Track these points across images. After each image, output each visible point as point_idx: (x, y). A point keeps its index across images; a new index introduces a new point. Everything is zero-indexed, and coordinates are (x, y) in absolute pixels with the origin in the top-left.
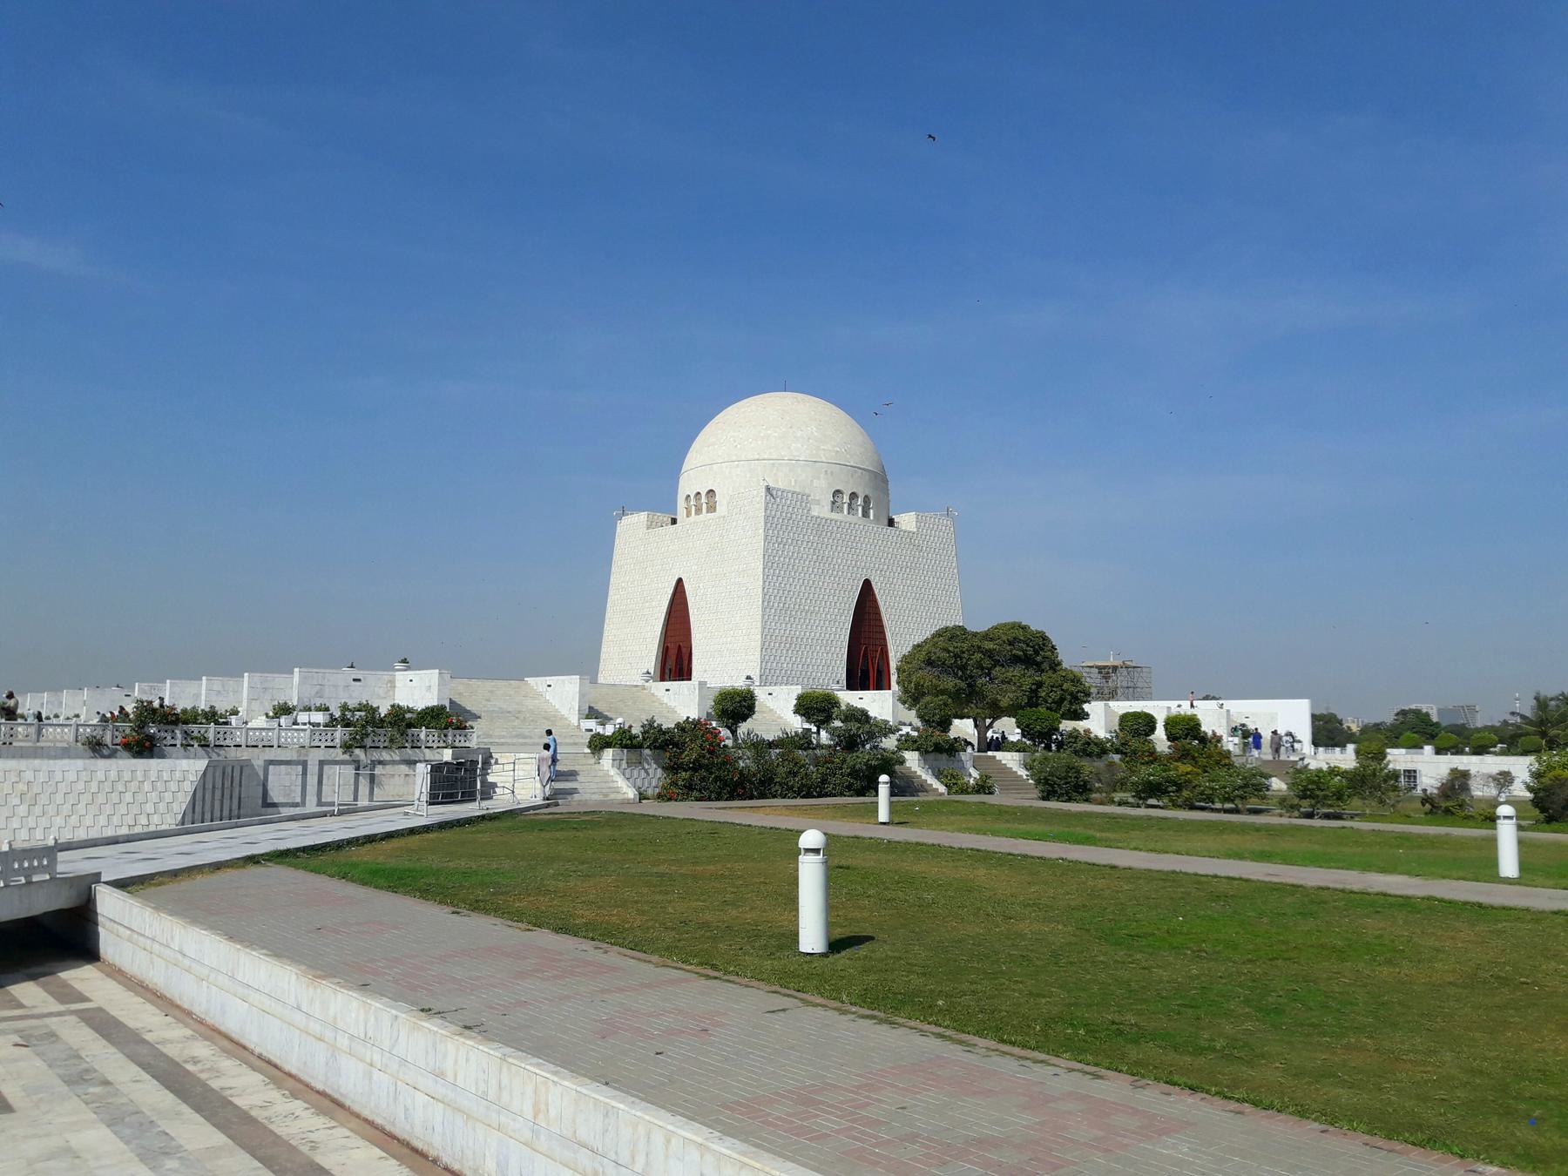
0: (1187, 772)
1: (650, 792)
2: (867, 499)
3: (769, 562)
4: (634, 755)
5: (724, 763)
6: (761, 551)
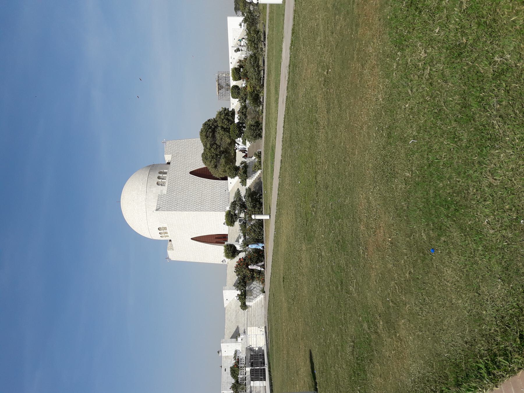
0: (251, 70)
1: (262, 286)
2: (160, 173)
3: (184, 209)
4: (248, 293)
5: (251, 259)
6: (180, 212)
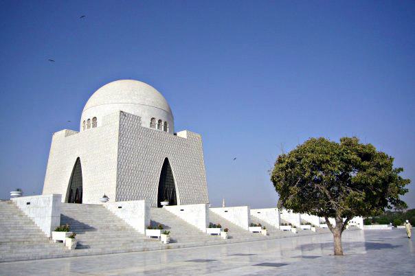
2: (165, 123)
